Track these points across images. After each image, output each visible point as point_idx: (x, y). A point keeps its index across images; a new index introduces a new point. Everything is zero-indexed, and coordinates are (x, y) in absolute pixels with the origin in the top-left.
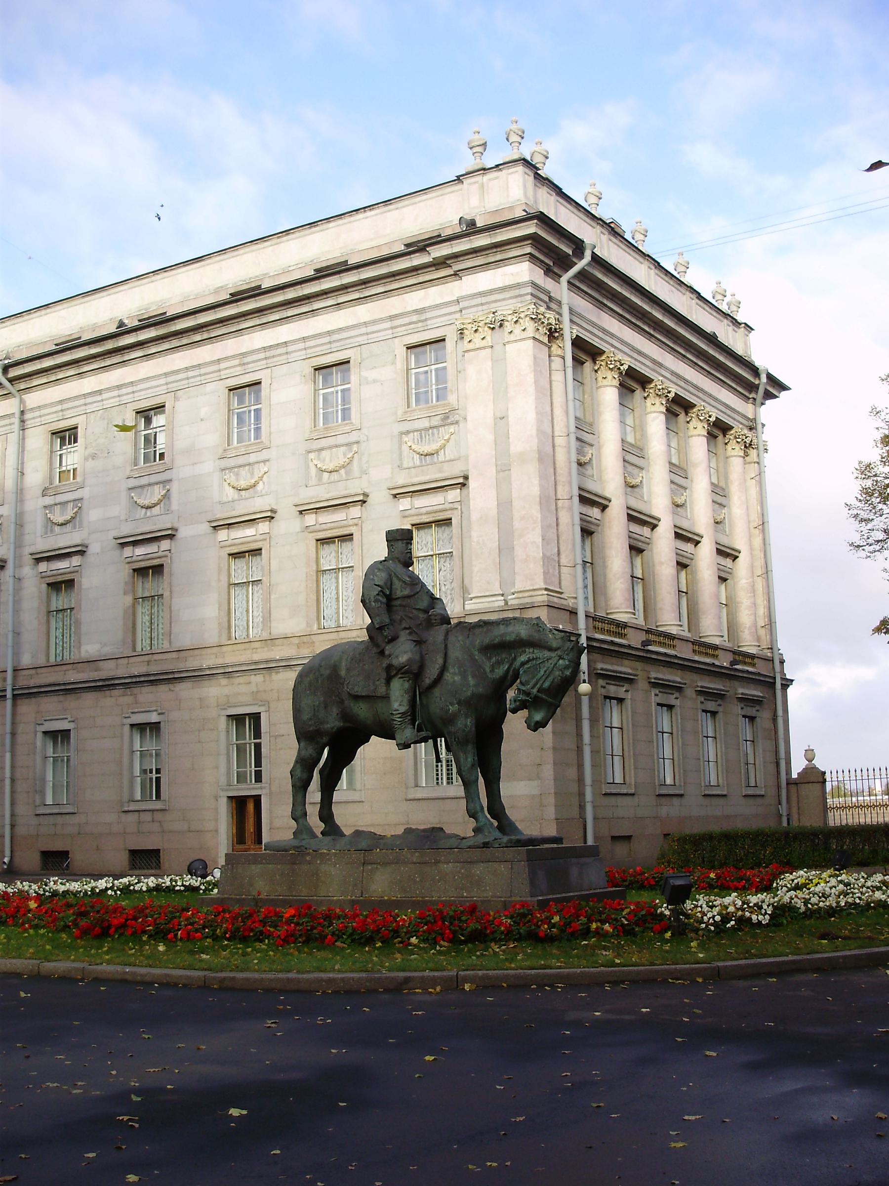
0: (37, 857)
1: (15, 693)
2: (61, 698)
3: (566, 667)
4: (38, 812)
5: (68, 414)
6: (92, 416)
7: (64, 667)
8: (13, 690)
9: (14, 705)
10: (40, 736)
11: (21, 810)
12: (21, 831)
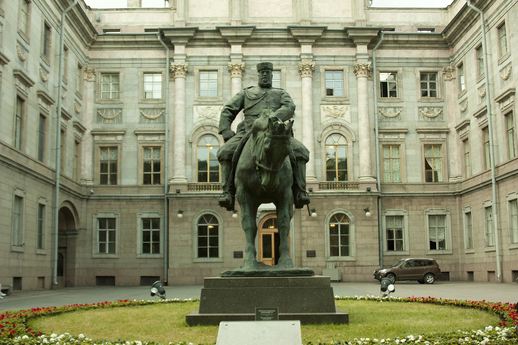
0: (511, 273)
1: (497, 180)
2: (513, 180)
3: (266, 142)
4: (510, 248)
5: (502, 14)
6: (509, 11)
7: (513, 162)
8: (496, 178)
9: (498, 188)
10: (508, 202)
11: (505, 247)
12: (506, 259)
